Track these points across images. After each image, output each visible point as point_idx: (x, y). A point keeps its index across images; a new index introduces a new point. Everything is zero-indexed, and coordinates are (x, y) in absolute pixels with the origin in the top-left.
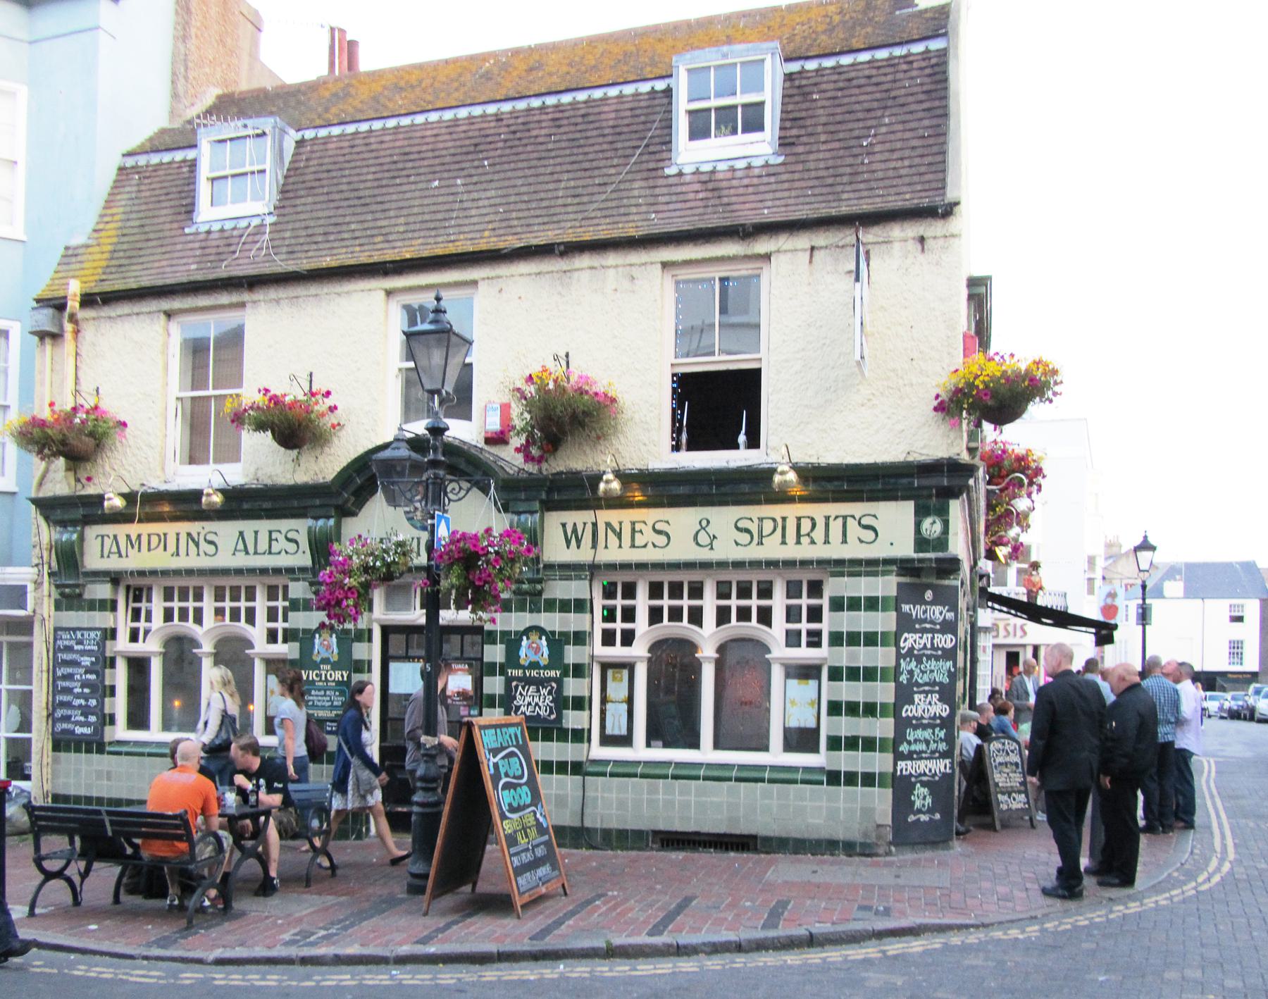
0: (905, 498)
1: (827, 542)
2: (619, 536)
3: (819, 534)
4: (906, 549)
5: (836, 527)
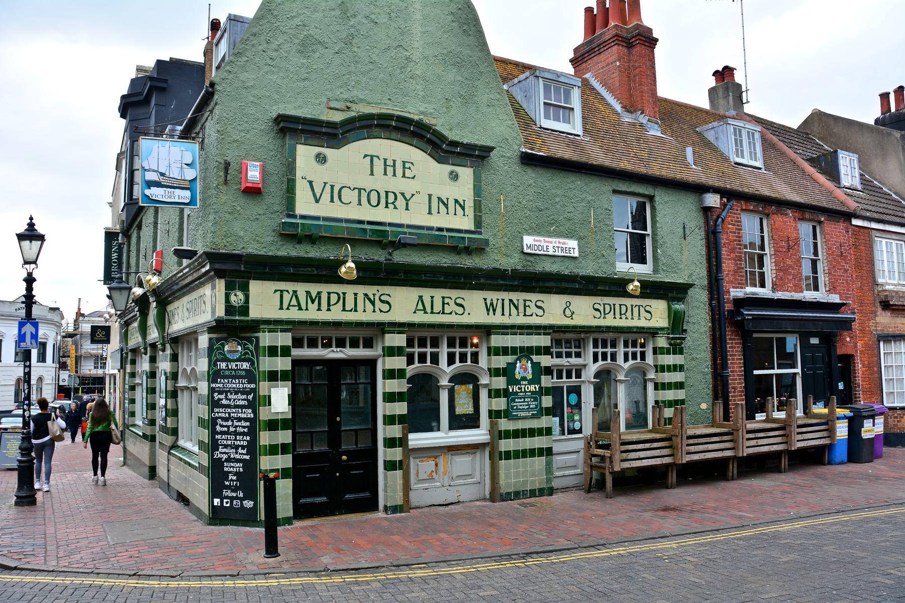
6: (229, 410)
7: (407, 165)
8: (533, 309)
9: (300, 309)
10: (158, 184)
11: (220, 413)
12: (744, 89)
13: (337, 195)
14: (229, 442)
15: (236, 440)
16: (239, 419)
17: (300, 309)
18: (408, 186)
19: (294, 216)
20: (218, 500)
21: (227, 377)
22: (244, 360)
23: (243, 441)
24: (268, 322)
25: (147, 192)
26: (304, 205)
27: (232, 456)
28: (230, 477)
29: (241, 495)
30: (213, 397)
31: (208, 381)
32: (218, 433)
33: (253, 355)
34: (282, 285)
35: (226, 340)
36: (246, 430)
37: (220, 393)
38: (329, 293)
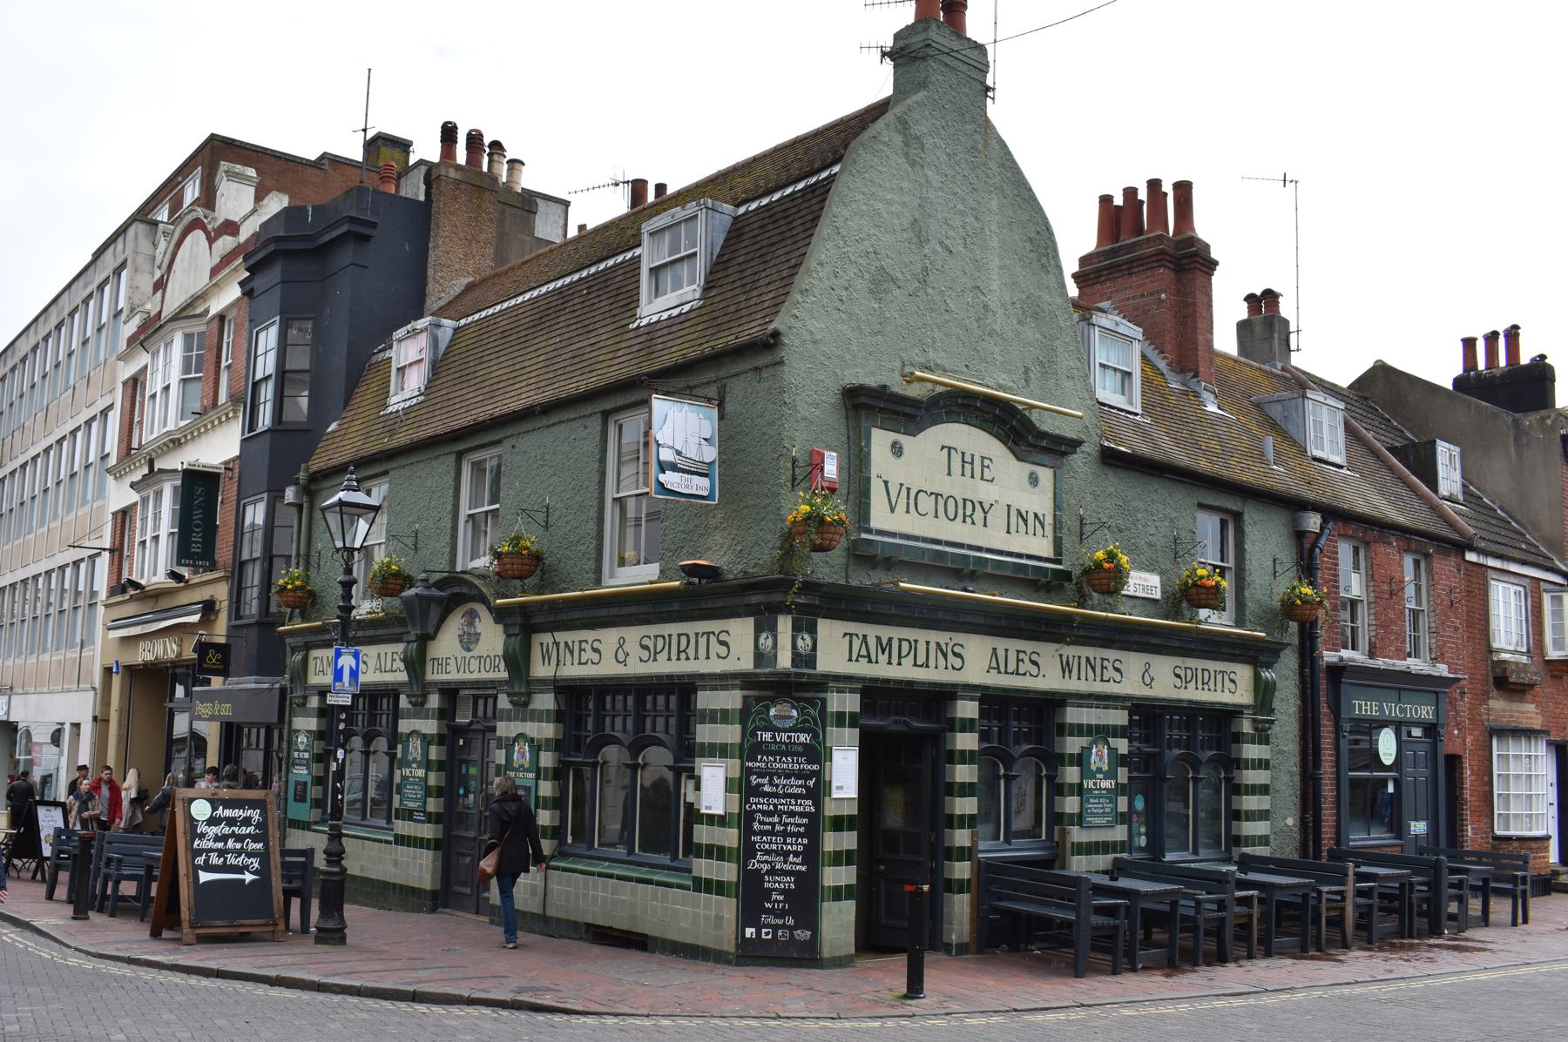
0: (748, 615)
1: (696, 658)
2: (572, 653)
4: (747, 664)
5: (702, 641)
8: (1109, 673)
9: (870, 661)
10: (674, 467)
12: (1293, 328)
13: (913, 499)
14: (774, 847)
15: (785, 843)
16: (792, 814)
18: (986, 492)
19: (870, 531)
21: (773, 753)
24: (837, 678)
25: (662, 478)
26: (880, 517)
29: (791, 922)
31: (741, 757)
32: (756, 834)
33: (816, 723)
34: (852, 627)
35: (773, 701)
37: (761, 775)
38: (900, 640)
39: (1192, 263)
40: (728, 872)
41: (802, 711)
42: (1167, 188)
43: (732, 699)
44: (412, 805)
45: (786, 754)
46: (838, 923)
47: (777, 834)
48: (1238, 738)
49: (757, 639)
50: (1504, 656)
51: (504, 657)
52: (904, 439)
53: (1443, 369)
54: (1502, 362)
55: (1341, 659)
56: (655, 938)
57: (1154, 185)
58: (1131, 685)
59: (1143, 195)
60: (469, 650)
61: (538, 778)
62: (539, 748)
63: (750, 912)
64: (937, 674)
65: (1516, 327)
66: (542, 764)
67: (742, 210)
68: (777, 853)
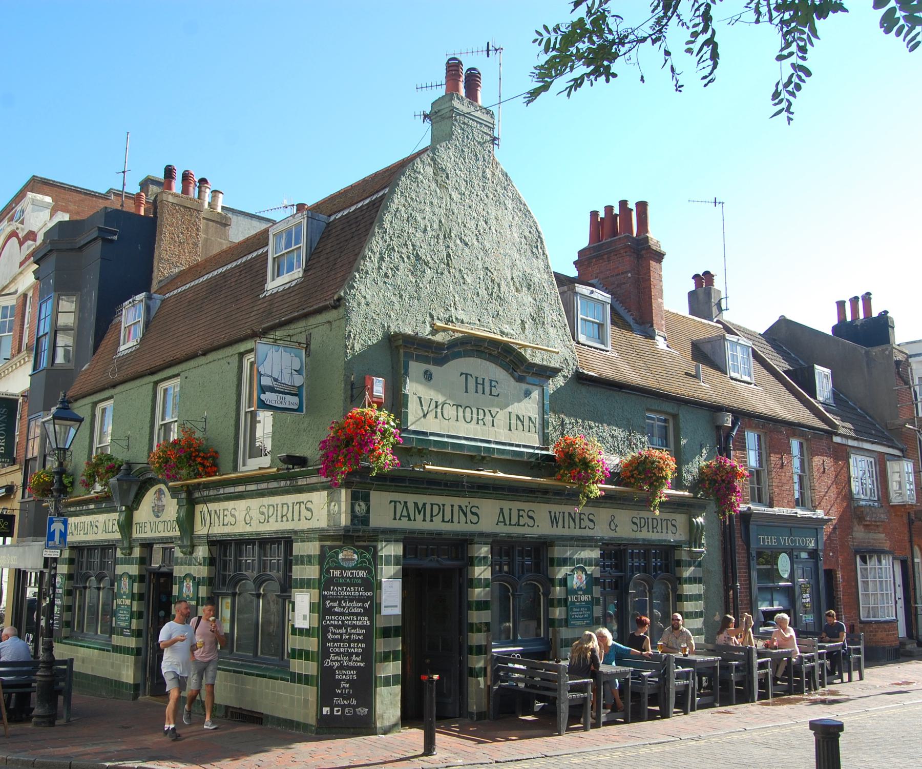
1: (293, 520)
3: (290, 515)
6: (343, 618)
7: (493, 384)
8: (586, 523)
10: (272, 390)
11: (333, 620)
12: (723, 295)
14: (342, 650)
17: (410, 519)
19: (406, 430)
20: (328, 709)
22: (361, 568)
23: (358, 648)
25: (263, 397)
27: (345, 664)
28: (342, 685)
29: (354, 702)
30: (324, 605)
31: (319, 589)
32: (329, 641)
36: (361, 637)
37: (333, 600)
38: (432, 505)
39: (645, 255)
40: (310, 668)
41: (361, 555)
42: (632, 205)
43: (312, 548)
44: (123, 624)
45: (348, 585)
46: (388, 702)
47: (344, 641)
48: (679, 563)
49: (329, 506)
50: (862, 503)
51: (177, 521)
52: (432, 368)
53: (823, 321)
54: (861, 316)
55: (749, 508)
56: (267, 716)
57: (623, 204)
58: (601, 531)
59: (616, 211)
60: (158, 517)
61: (198, 604)
62: (199, 585)
63: (325, 698)
64: (460, 526)
65: (868, 294)
66: (200, 595)
67: (332, 218)
68: (344, 654)
